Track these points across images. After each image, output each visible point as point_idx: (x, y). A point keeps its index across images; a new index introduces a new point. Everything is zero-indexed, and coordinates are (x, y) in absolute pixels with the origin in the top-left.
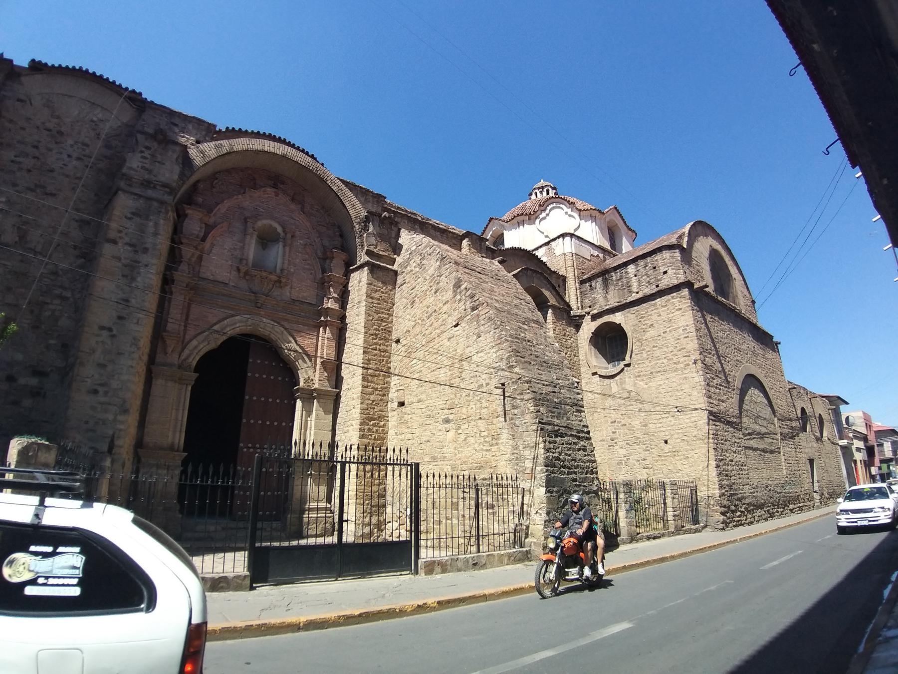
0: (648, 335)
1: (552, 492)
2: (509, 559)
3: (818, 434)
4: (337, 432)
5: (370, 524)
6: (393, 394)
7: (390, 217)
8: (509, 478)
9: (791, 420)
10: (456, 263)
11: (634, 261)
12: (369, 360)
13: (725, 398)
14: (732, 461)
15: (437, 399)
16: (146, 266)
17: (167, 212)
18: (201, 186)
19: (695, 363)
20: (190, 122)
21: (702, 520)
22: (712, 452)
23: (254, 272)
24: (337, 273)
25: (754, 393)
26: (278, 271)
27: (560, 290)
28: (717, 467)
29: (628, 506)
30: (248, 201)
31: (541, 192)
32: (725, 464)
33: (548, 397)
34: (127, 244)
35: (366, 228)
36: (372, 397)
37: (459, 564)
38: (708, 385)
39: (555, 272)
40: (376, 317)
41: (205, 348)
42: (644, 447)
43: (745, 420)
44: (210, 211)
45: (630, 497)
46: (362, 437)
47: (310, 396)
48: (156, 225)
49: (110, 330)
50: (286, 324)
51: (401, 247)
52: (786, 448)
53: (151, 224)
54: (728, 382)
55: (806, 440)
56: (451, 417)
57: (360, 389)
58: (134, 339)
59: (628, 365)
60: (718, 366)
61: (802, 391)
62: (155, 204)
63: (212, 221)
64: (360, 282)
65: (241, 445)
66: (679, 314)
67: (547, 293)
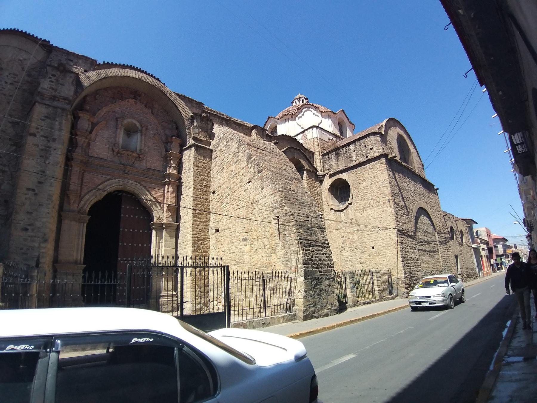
0: (362, 186)
1: (307, 279)
2: (284, 319)
3: (460, 241)
4: (179, 249)
5: (200, 303)
6: (212, 225)
7: (207, 116)
8: (283, 272)
9: (445, 233)
10: (248, 144)
11: (354, 142)
12: (197, 204)
13: (406, 221)
14: (411, 258)
15: (239, 227)
16: (55, 150)
17: (67, 116)
18: (88, 99)
19: (389, 201)
20: (80, 58)
21: (395, 292)
22: (400, 253)
24: (175, 151)
25: (423, 219)
26: (138, 151)
27: (311, 160)
28: (403, 261)
29: (352, 285)
30: (117, 107)
31: (299, 101)
32: (407, 260)
33: (305, 224)
34: (42, 136)
35: (192, 124)
36: (199, 227)
37: (254, 324)
38: (397, 214)
39: (307, 149)
40: (200, 178)
41: (94, 200)
42: (361, 251)
43: (418, 234)
44: (94, 114)
45: (353, 280)
46: (194, 251)
47: (160, 228)
48: (60, 124)
49: (33, 190)
50: (144, 184)
51: (214, 135)
52: (442, 250)
53: (57, 123)
54: (408, 212)
55: (453, 245)
56: (247, 237)
57: (192, 222)
59: (351, 204)
60: (402, 203)
61: (451, 217)
62: (59, 110)
63: (95, 121)
64: (189, 157)
65: (119, 259)
66: (380, 173)
67: (303, 162)
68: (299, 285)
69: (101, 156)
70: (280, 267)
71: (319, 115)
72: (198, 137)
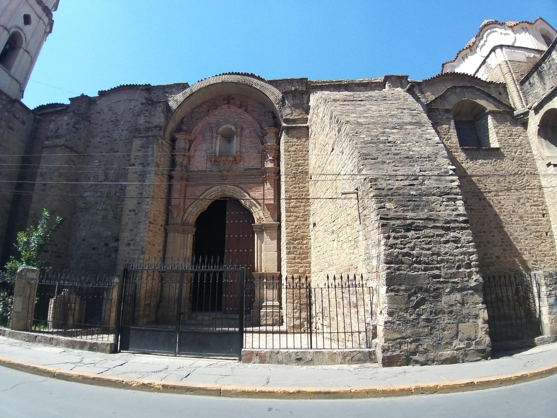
5: (300, 318)
17: (158, 140)
23: (219, 160)
24: (270, 143)
27: (501, 98)
30: (212, 119)
33: (401, 192)
35: (284, 104)
36: (295, 223)
37: (280, 357)
39: (491, 83)
40: (294, 164)
46: (289, 253)
47: (263, 229)
49: (134, 211)
56: (334, 228)
58: (146, 213)
62: (151, 138)
63: (193, 137)
67: (482, 102)
68: (381, 300)
70: (362, 270)
71: (509, 32)
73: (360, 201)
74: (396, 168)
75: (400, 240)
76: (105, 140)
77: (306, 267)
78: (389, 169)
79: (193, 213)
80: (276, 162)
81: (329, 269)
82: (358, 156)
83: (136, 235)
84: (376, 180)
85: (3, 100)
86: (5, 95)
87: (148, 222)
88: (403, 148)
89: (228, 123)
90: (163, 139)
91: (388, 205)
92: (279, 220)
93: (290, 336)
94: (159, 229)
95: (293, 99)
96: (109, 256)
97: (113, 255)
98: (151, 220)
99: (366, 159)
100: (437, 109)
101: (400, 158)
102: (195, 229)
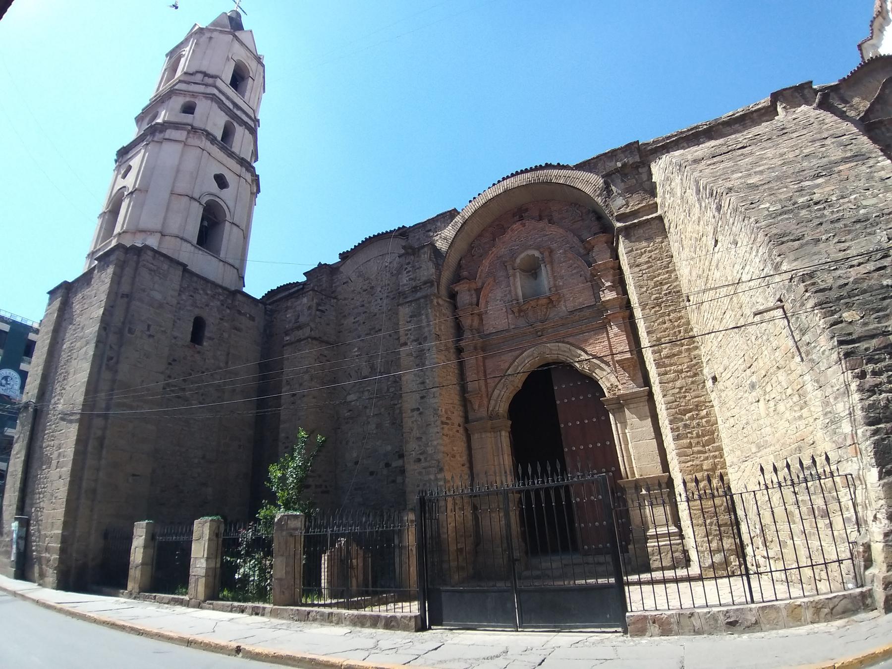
17: (432, 301)
20: (437, 221)
23: (525, 307)
24: (602, 259)
30: (501, 249)
33: (865, 286)
36: (678, 384)
40: (651, 283)
47: (621, 403)
49: (418, 409)
50: (571, 340)
53: (424, 317)
56: (754, 379)
62: (422, 300)
63: (479, 285)
69: (500, 328)
70: (825, 445)
72: (628, 210)
73: (793, 320)
74: (843, 245)
75: (885, 375)
76: (360, 319)
77: (715, 457)
78: (831, 250)
79: (501, 398)
80: (620, 288)
81: (759, 454)
82: (766, 242)
83: (427, 445)
84: (811, 275)
85: (219, 294)
86: (221, 287)
87: (439, 423)
88: (845, 206)
89: (527, 248)
90: (438, 297)
91: (847, 316)
92: (647, 382)
93: (710, 585)
94: (458, 431)
95: (623, 181)
96: (394, 481)
97: (399, 479)
98: (444, 419)
99: (783, 243)
100: (881, 122)
101: (845, 226)
102: (510, 422)
